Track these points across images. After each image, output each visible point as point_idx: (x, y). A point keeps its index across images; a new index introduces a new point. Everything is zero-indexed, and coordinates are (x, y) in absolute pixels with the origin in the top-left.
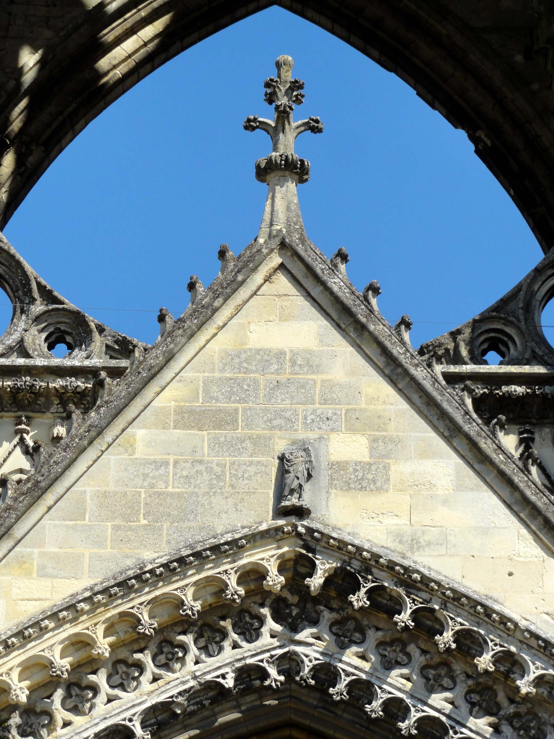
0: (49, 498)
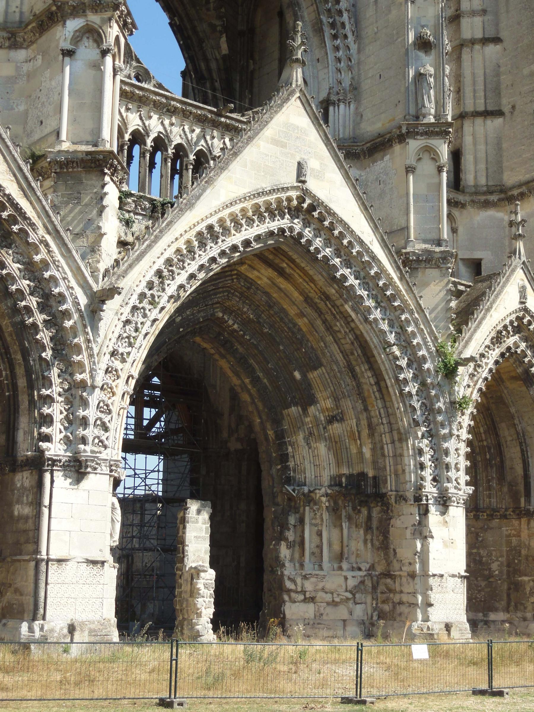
0: (238, 158)
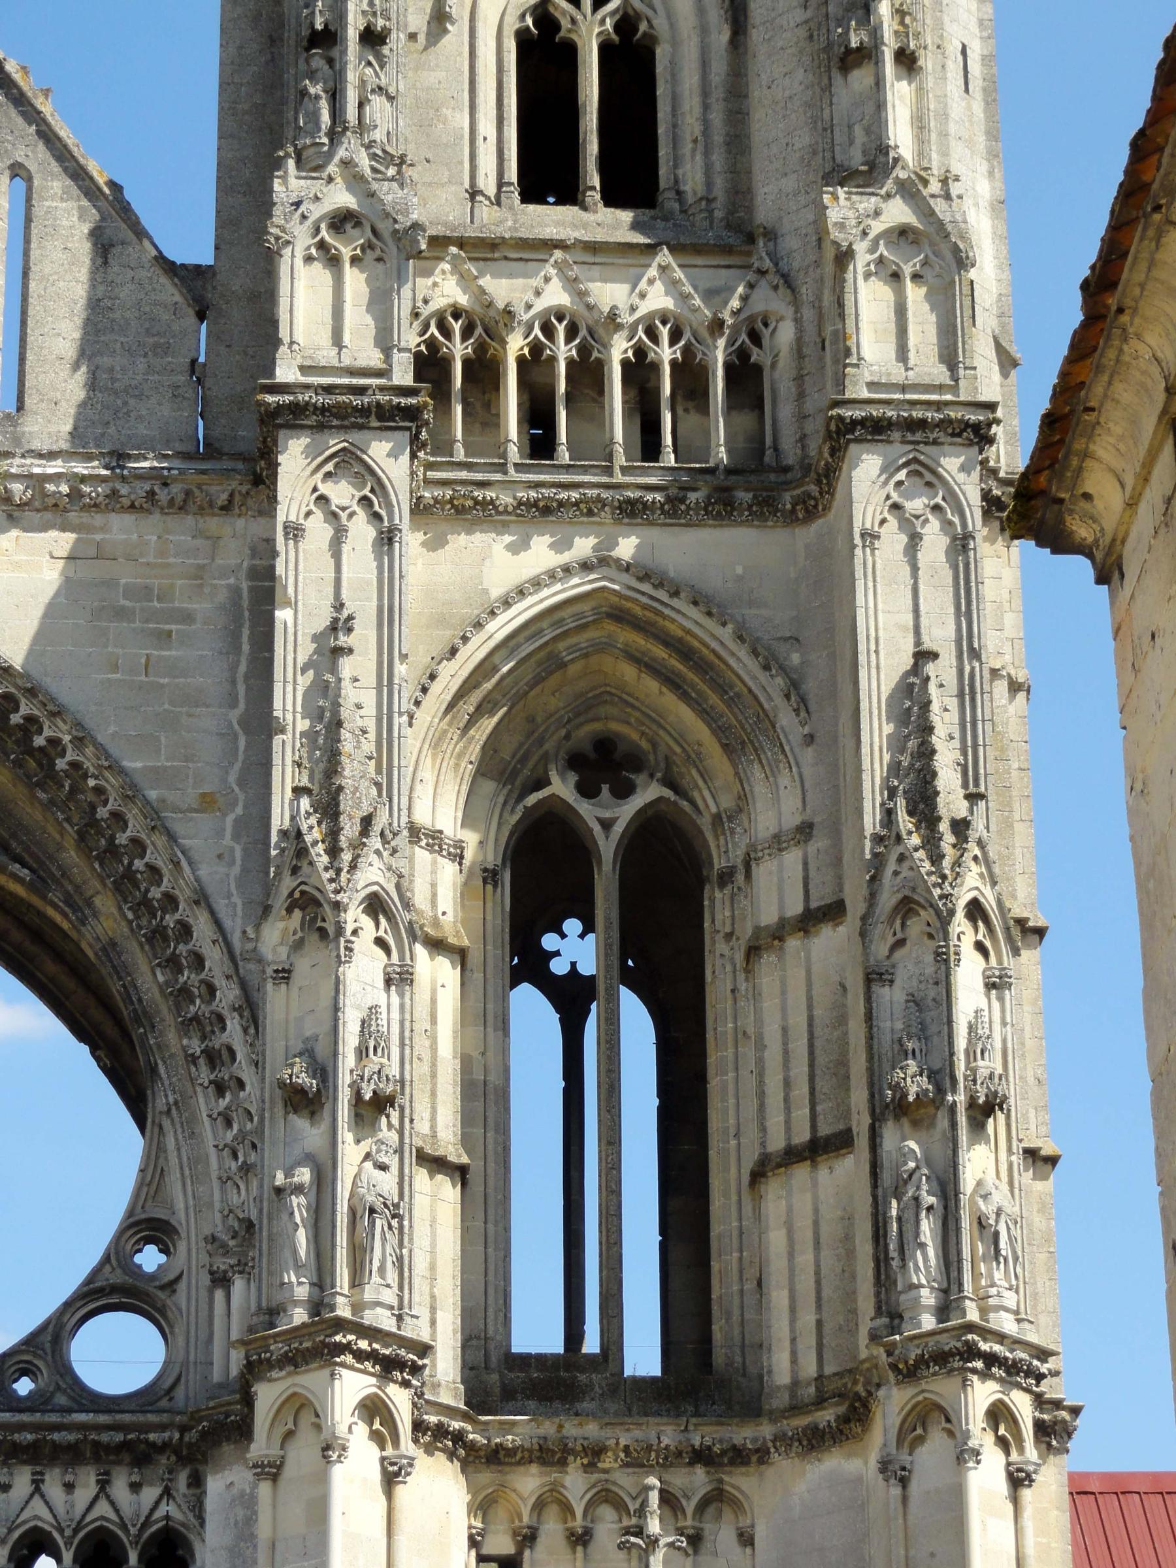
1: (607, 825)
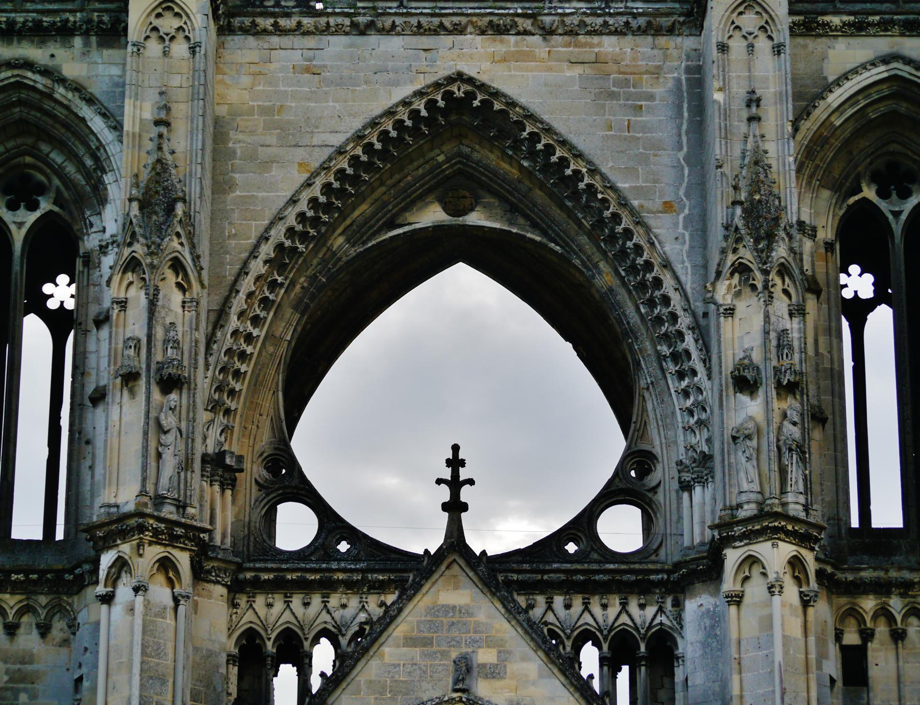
0: (344, 685)
1: (897, 214)
